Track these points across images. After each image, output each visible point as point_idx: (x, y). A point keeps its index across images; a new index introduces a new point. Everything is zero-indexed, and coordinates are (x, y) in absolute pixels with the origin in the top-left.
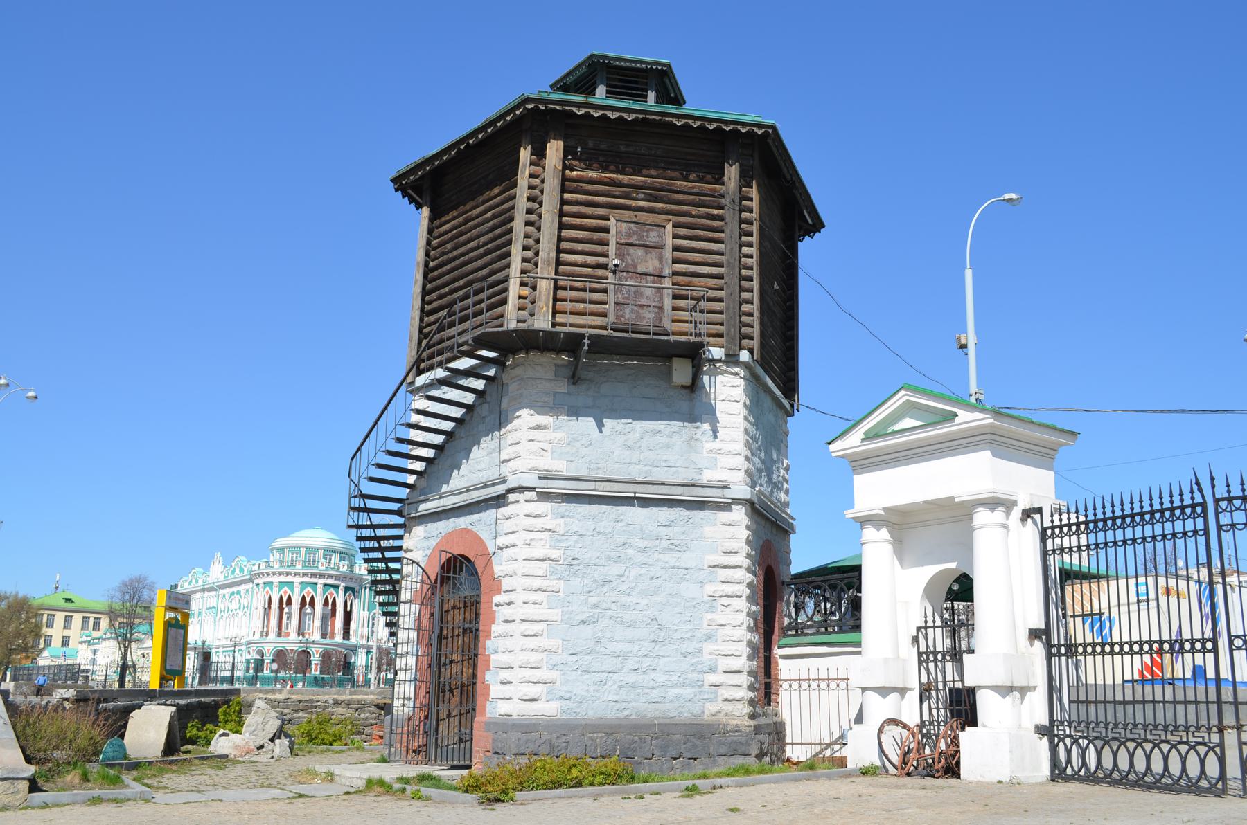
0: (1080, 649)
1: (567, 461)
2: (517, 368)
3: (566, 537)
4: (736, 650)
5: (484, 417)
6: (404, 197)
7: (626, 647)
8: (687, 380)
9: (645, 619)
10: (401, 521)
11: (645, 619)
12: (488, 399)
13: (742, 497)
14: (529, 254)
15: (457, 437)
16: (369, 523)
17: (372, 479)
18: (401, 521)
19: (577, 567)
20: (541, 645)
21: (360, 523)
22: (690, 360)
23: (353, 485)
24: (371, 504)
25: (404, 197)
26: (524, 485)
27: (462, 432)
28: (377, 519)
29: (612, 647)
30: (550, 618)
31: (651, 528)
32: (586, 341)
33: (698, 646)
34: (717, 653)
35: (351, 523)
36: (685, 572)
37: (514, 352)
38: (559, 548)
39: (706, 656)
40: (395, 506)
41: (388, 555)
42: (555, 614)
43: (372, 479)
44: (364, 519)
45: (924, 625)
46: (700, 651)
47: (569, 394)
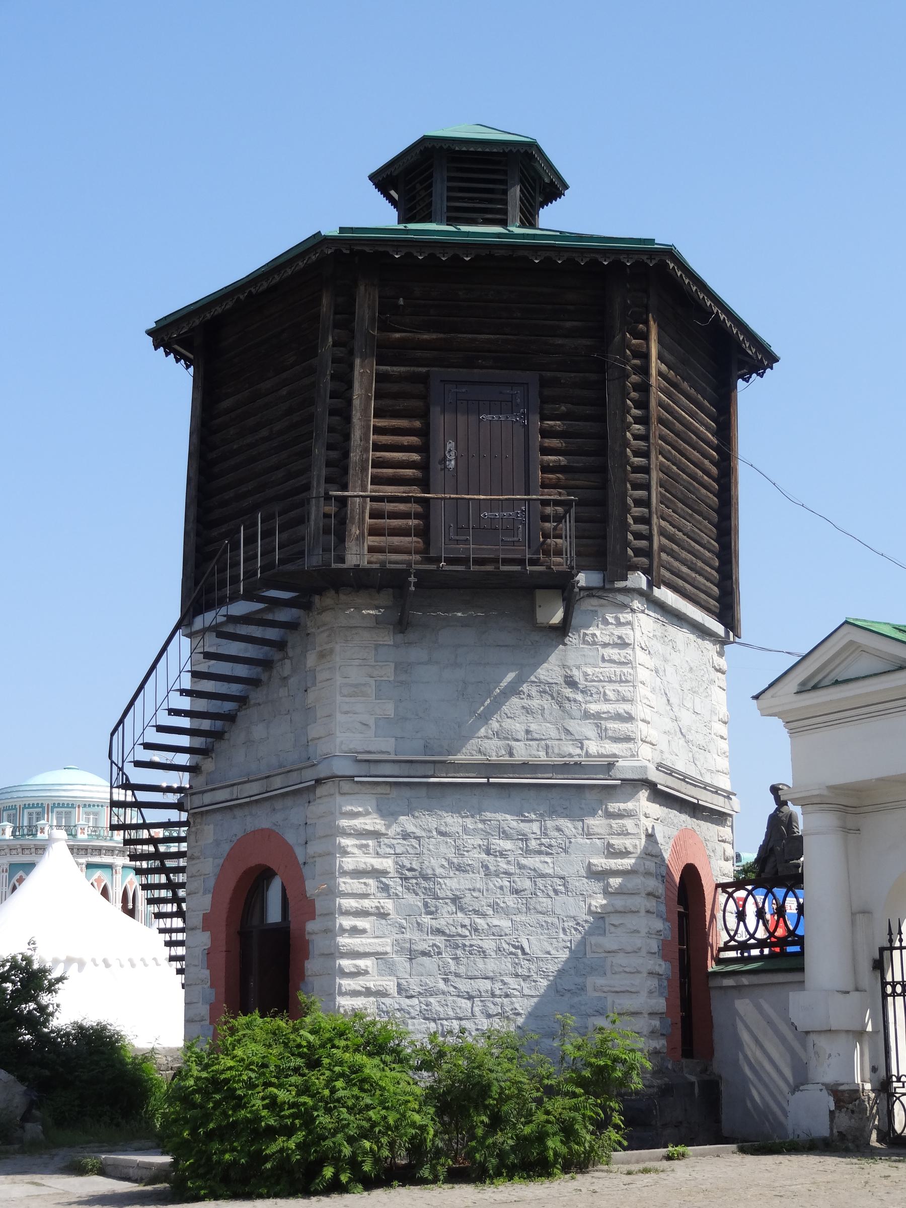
0: (899, 989)
1: (396, 738)
2: (324, 614)
3: (399, 841)
4: (633, 985)
5: (285, 678)
6: (167, 354)
7: (486, 985)
8: (558, 617)
9: (506, 946)
10: (184, 816)
11: (506, 946)
12: (290, 654)
13: (636, 777)
14: (334, 455)
15: (252, 702)
16: (141, 821)
17: (138, 764)
18: (184, 816)
19: (414, 881)
20: (371, 985)
21: (128, 822)
22: (560, 591)
23: (115, 768)
24: (143, 796)
25: (167, 354)
26: (340, 774)
27: (256, 696)
28: (152, 816)
29: (464, 986)
30: (380, 949)
31: (514, 824)
32: (412, 579)
33: (579, 980)
34: (605, 989)
35: (115, 821)
36: (558, 881)
37: (320, 591)
38: (386, 856)
39: (591, 993)
40: (172, 798)
41: (170, 863)
42: (385, 945)
43: (138, 764)
44: (132, 816)
45: (888, 945)
46: (583, 989)
47: (396, 646)
